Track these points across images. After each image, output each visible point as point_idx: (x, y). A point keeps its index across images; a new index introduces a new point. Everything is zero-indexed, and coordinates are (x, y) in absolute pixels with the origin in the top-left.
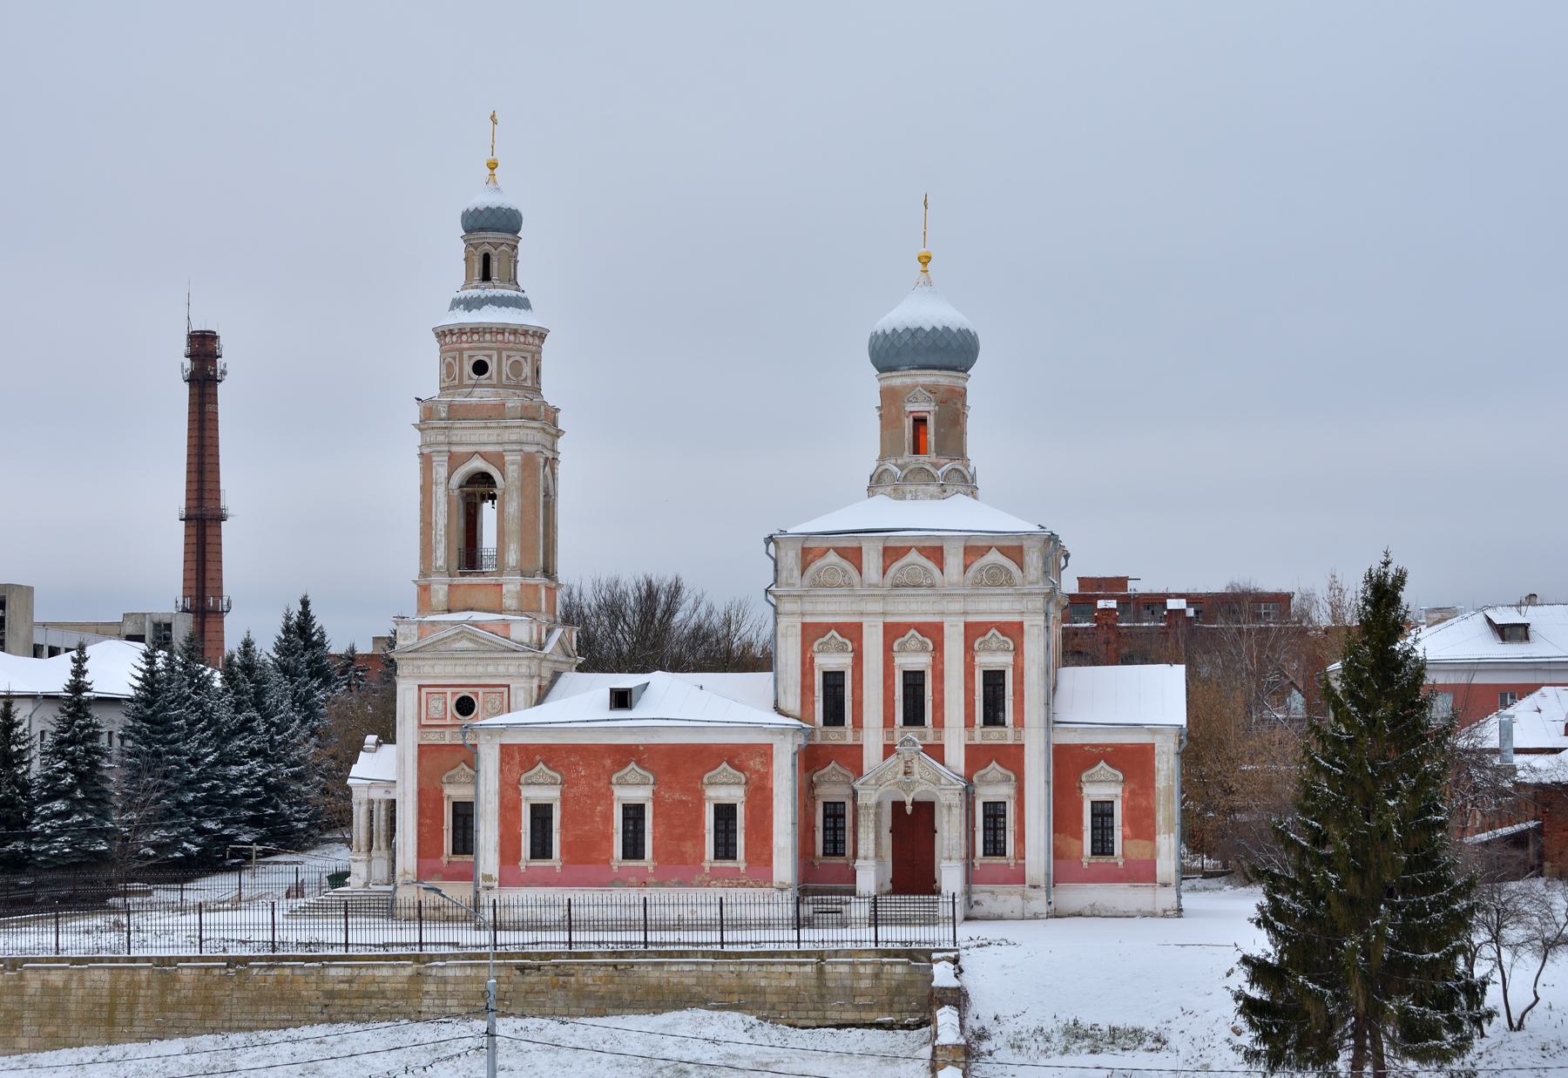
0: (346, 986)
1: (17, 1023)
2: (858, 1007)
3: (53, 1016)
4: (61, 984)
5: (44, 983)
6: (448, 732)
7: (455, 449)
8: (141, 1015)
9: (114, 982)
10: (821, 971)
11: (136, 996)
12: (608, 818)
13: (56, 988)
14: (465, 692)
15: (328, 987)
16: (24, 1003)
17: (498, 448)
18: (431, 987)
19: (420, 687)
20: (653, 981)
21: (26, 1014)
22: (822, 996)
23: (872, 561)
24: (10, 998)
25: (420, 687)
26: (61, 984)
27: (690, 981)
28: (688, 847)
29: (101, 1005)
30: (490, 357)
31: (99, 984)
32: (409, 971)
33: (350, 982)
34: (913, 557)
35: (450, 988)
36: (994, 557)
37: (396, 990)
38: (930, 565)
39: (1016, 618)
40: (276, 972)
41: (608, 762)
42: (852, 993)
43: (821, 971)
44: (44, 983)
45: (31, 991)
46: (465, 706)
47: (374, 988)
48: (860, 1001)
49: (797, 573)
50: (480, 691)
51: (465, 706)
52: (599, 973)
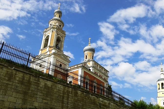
1: (35, 96)
3: (47, 96)
4: (50, 86)
5: (45, 84)
7: (58, 33)
8: (70, 101)
9: (64, 89)
11: (69, 95)
13: (49, 87)
14: (61, 63)
16: (38, 89)
17: (62, 36)
19: (56, 60)
21: (39, 93)
24: (34, 86)
26: (50, 86)
29: (61, 96)
31: (60, 89)
34: (101, 68)
36: (105, 72)
40: (93, 96)
44: (45, 84)
45: (41, 86)
46: (61, 65)
50: (63, 64)
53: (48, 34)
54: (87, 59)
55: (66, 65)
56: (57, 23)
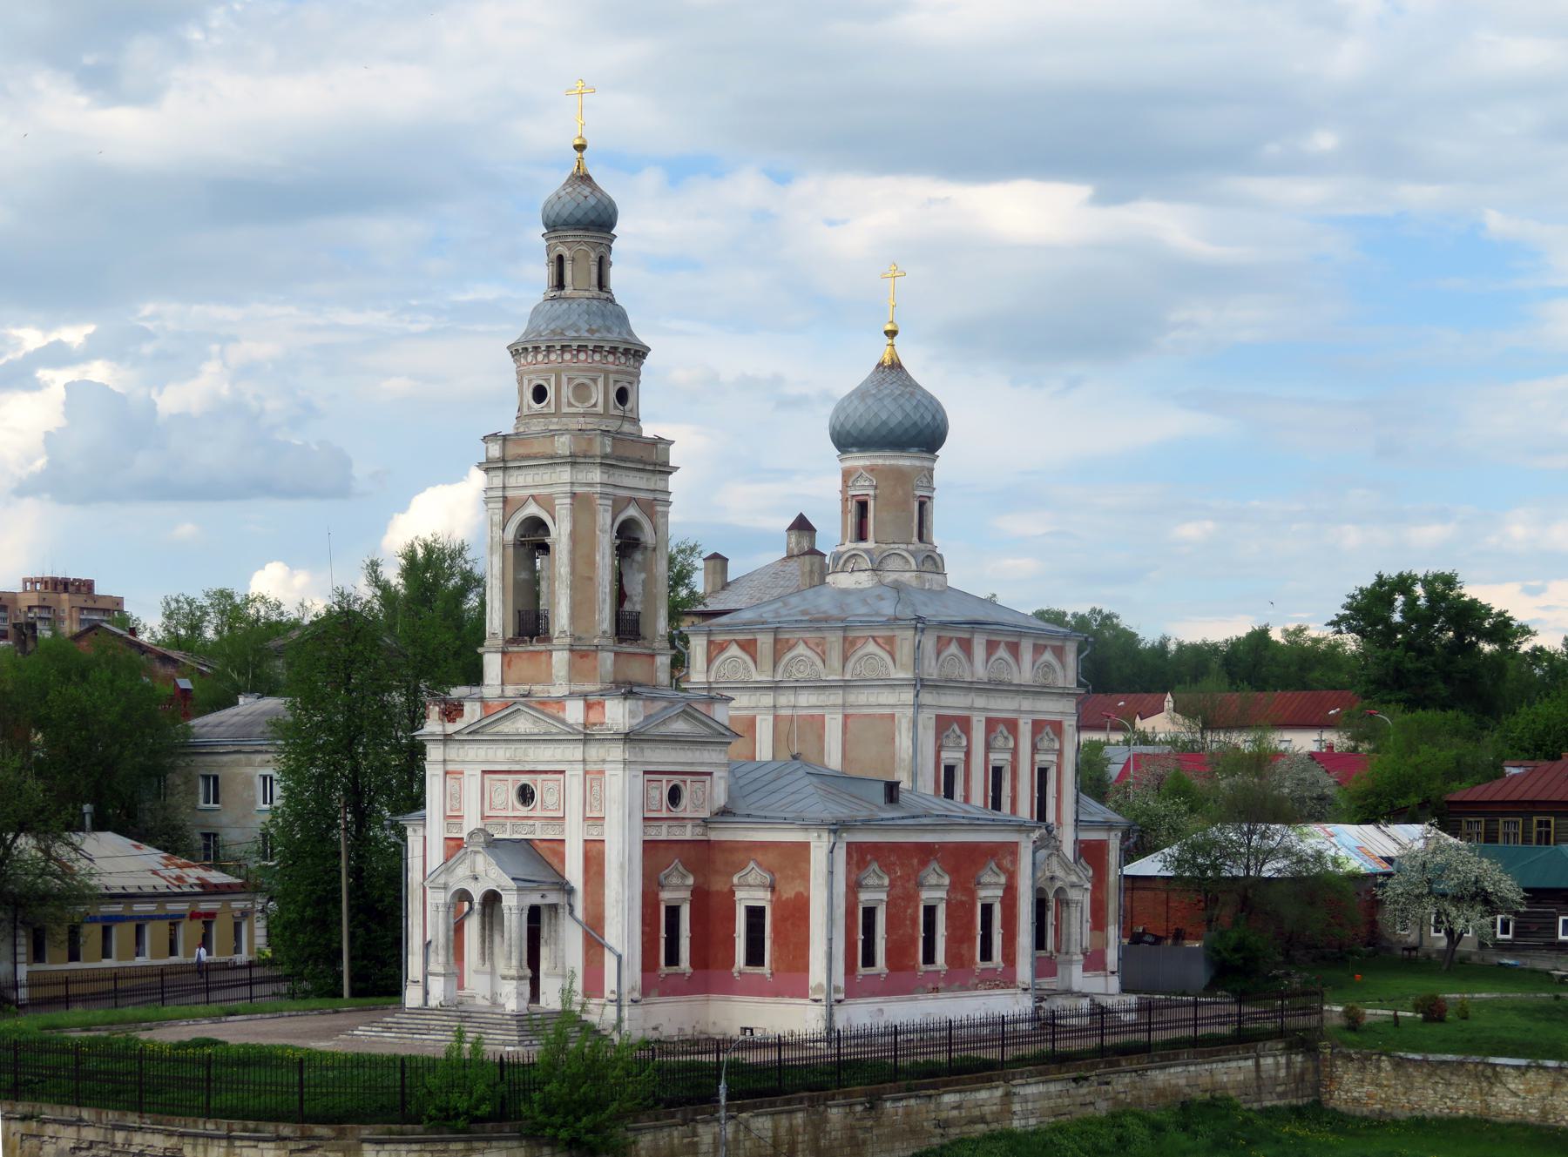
0: (955, 1113)
2: (1281, 1096)
6: (665, 825)
9: (775, 1129)
10: (1258, 1065)
12: (915, 921)
14: (676, 780)
15: (944, 1115)
17: (650, 496)
18: (1017, 1107)
20: (1160, 1084)
22: (1259, 1087)
23: (979, 651)
25: (645, 772)
27: (1182, 1082)
28: (964, 949)
30: (547, 380)
32: (999, 1093)
33: (958, 1107)
34: (1002, 652)
35: (1030, 1106)
36: (1048, 656)
37: (992, 1113)
38: (1011, 660)
39: (1058, 718)
40: (904, 1103)
41: (915, 861)
42: (1275, 1081)
43: (1258, 1065)
46: (675, 796)
47: (976, 1112)
48: (1280, 1089)
49: (933, 662)
50: (689, 779)
51: (675, 796)
52: (1127, 1080)
53: (533, 510)
54: (870, 544)
55: (710, 774)
56: (594, 380)
